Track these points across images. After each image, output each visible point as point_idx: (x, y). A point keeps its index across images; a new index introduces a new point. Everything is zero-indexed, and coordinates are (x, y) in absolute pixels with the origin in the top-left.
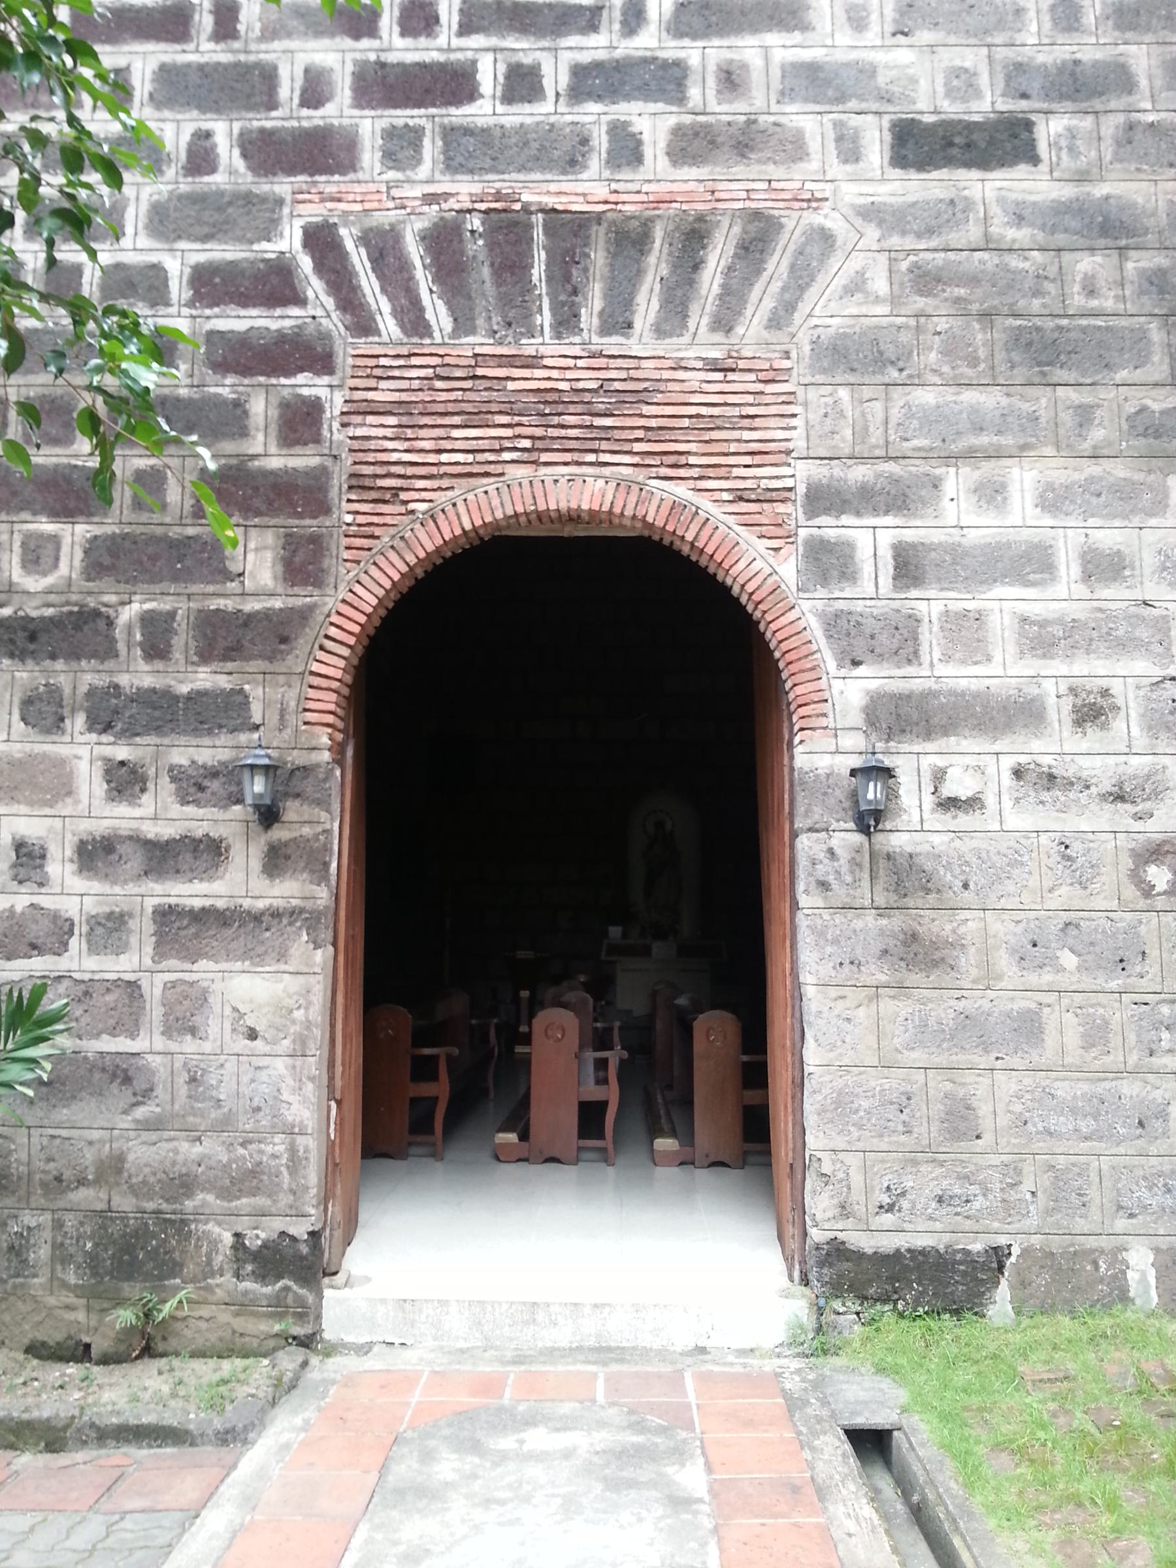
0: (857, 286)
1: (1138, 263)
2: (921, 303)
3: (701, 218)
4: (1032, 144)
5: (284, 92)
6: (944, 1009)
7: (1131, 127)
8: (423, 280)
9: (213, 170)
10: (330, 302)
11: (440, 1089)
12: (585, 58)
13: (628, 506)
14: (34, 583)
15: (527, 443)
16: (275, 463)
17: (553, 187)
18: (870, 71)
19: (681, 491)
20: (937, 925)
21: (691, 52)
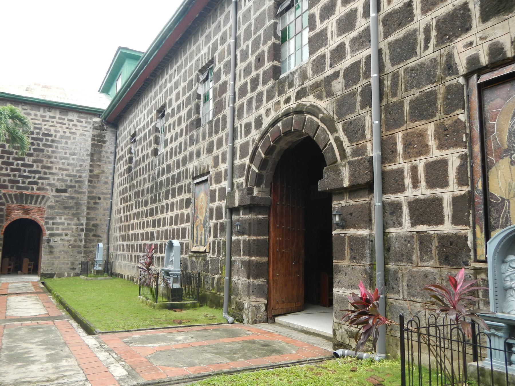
0: (51, 202)
1: (74, 201)
6: (53, 256)
8: (14, 199)
11: (12, 267)
13: (30, 218)
18: (54, 184)
20: (53, 250)
21: (39, 181)
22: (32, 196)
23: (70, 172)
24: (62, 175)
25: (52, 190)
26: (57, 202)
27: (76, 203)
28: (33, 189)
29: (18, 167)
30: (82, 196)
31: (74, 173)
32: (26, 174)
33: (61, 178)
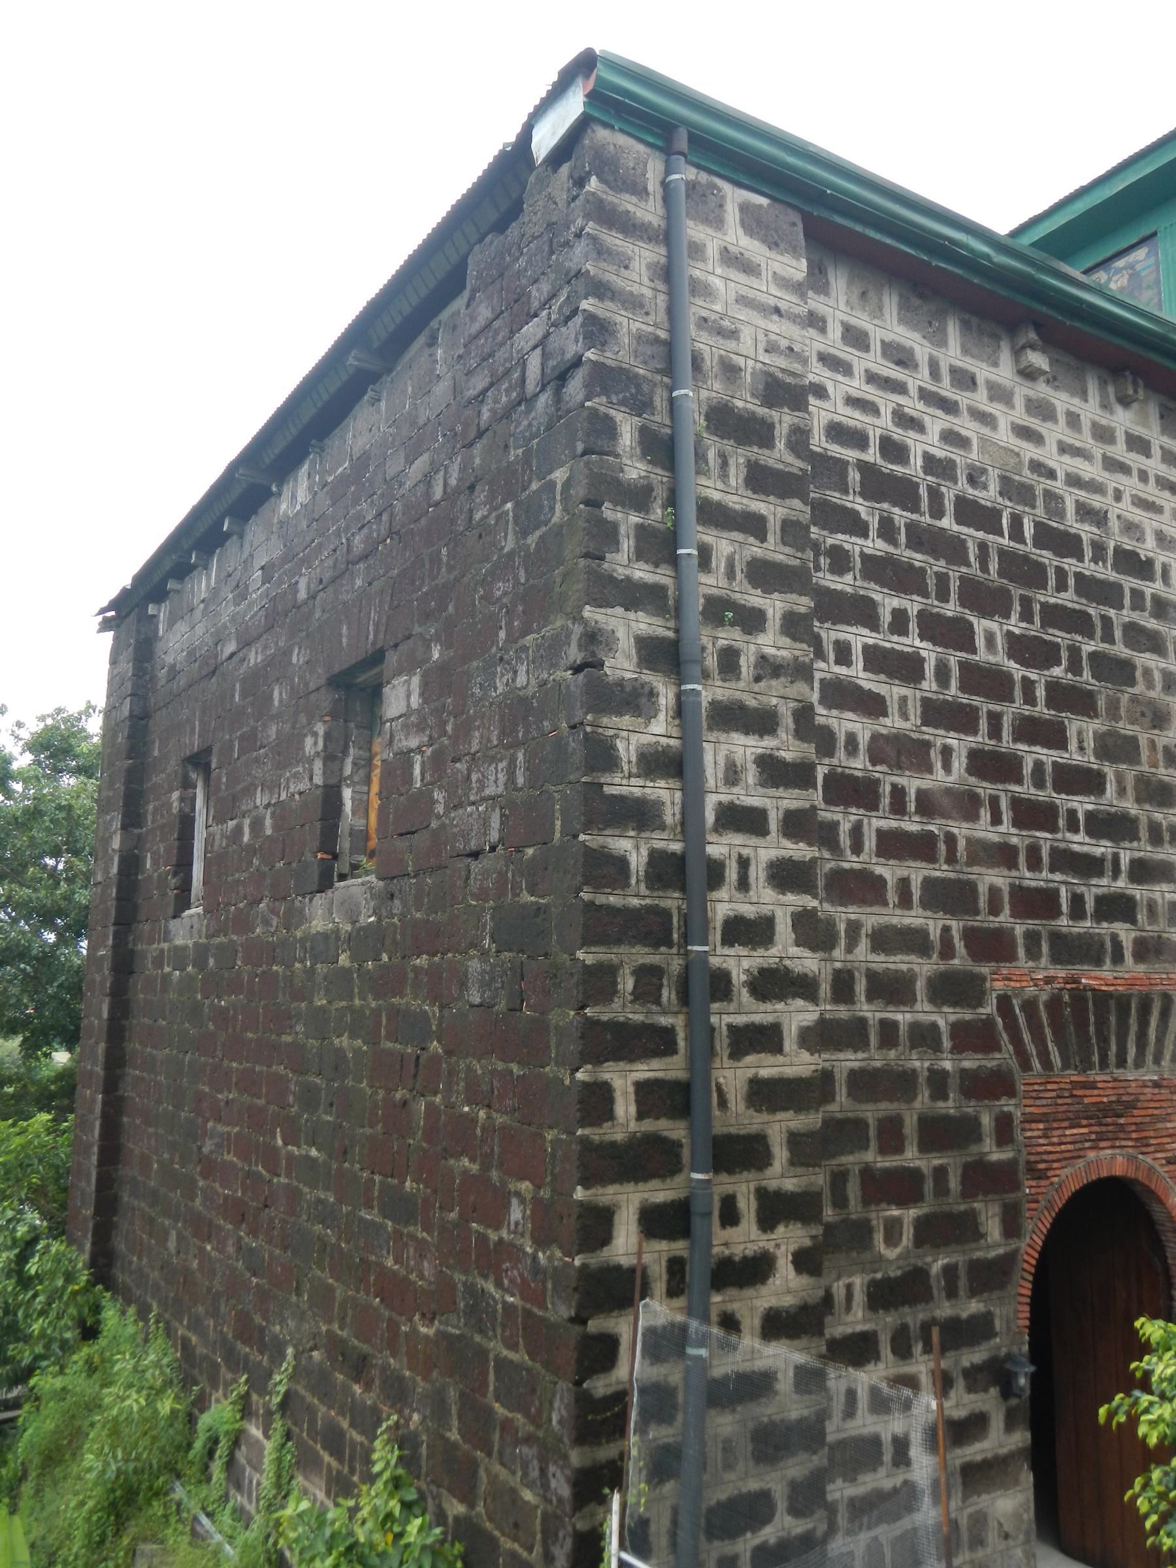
8: (1048, 1031)
9: (953, 957)
10: (1011, 1048)
12: (1100, 891)
15: (1093, 1137)
16: (995, 1157)
17: (1093, 974)
21: (1138, 892)
22: (1123, 1004)
32: (1080, 842)
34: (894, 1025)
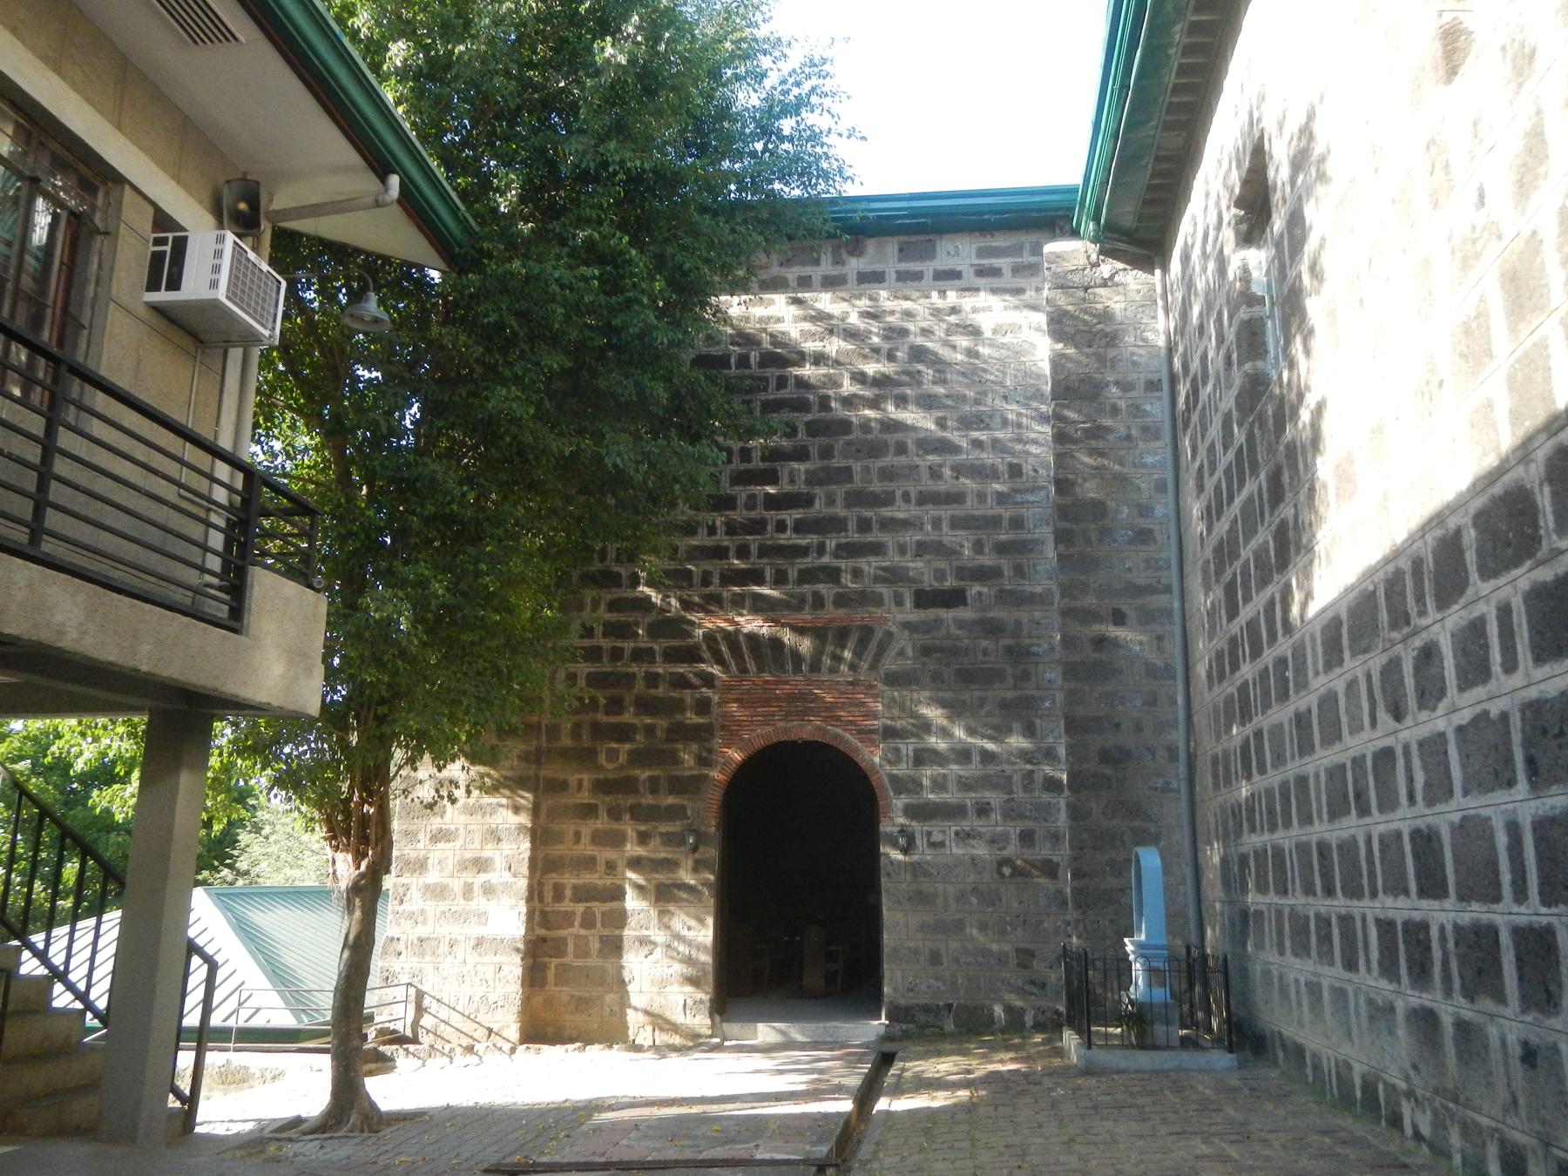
0: (902, 653)
1: (1005, 642)
2: (925, 659)
3: (844, 628)
4: (965, 598)
5: (695, 581)
7: (1001, 591)
12: (803, 567)
14: (610, 766)
19: (838, 730)
21: (842, 564)
23: (970, 507)
24: (937, 523)
25: (899, 601)
26: (927, 651)
27: (1009, 650)
28: (819, 602)
29: (753, 514)
30: (1037, 615)
31: (991, 509)
32: (788, 538)
33: (934, 537)
34: (622, 649)
